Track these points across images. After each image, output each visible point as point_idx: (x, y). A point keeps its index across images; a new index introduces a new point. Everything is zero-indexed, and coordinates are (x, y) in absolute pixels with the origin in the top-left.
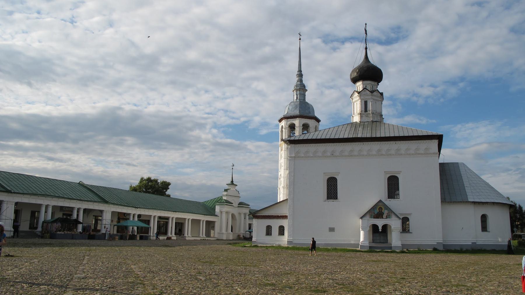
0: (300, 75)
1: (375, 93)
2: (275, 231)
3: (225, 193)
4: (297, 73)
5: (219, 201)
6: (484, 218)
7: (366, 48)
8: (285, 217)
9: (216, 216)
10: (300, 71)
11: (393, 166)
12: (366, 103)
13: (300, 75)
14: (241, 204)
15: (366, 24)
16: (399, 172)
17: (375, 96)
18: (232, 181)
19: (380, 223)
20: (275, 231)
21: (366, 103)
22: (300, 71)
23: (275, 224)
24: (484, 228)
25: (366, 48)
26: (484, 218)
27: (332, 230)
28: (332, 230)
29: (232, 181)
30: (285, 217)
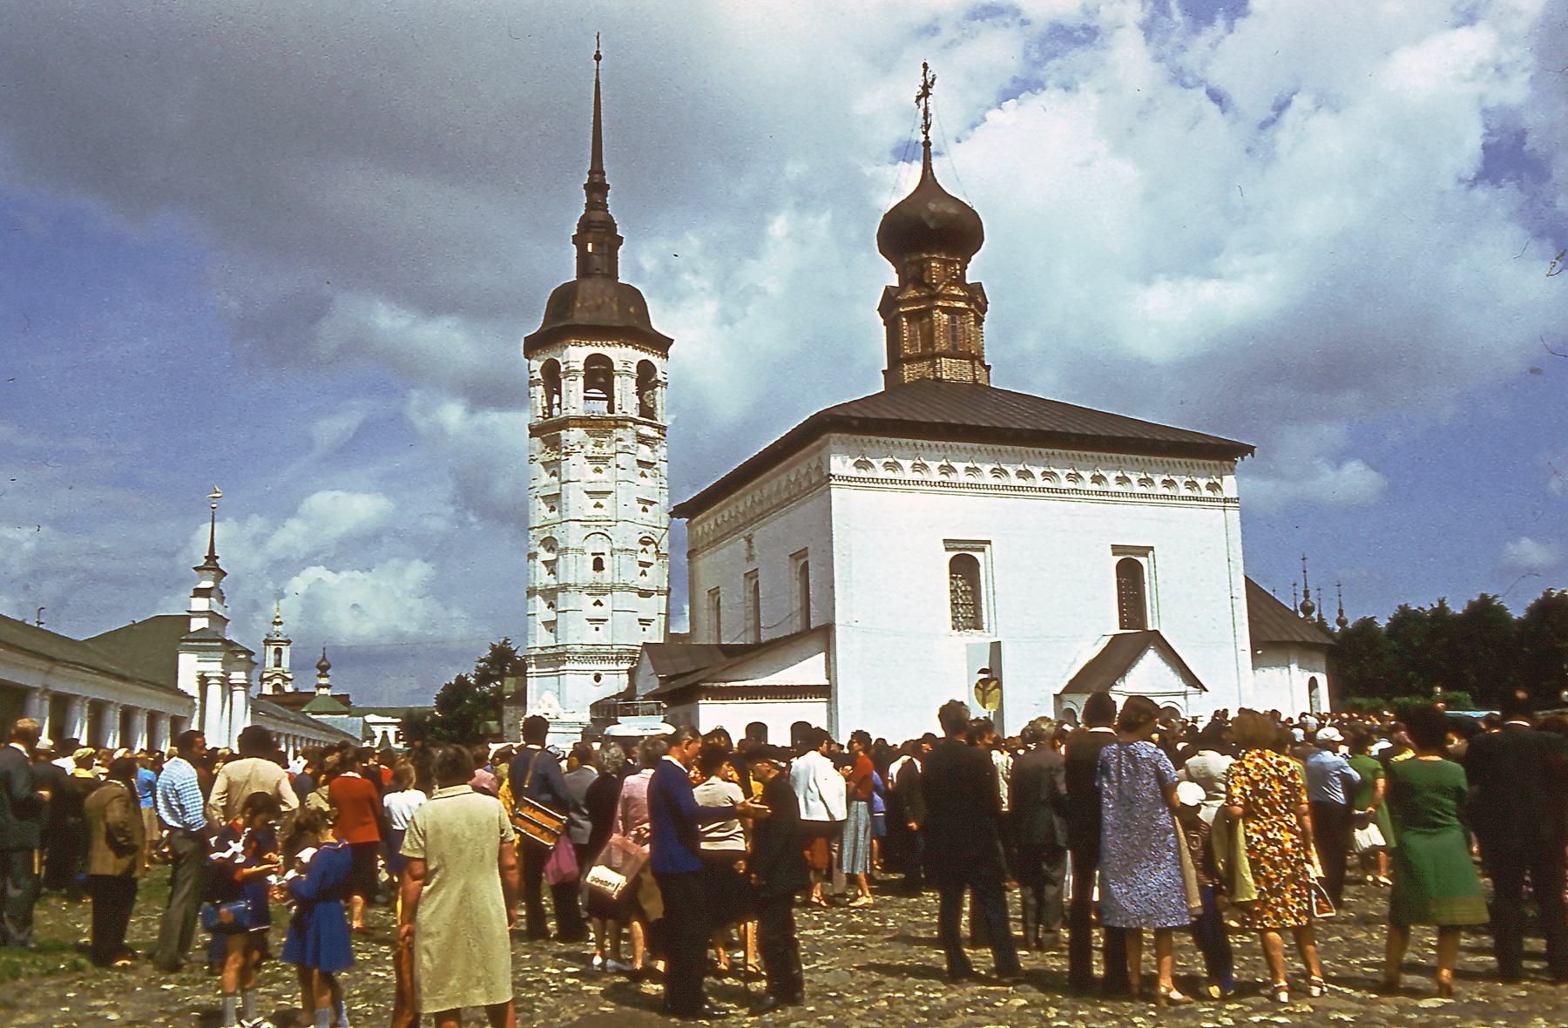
0: (597, 188)
13: (597, 188)
16: (1145, 551)
18: (212, 557)
29: (212, 557)
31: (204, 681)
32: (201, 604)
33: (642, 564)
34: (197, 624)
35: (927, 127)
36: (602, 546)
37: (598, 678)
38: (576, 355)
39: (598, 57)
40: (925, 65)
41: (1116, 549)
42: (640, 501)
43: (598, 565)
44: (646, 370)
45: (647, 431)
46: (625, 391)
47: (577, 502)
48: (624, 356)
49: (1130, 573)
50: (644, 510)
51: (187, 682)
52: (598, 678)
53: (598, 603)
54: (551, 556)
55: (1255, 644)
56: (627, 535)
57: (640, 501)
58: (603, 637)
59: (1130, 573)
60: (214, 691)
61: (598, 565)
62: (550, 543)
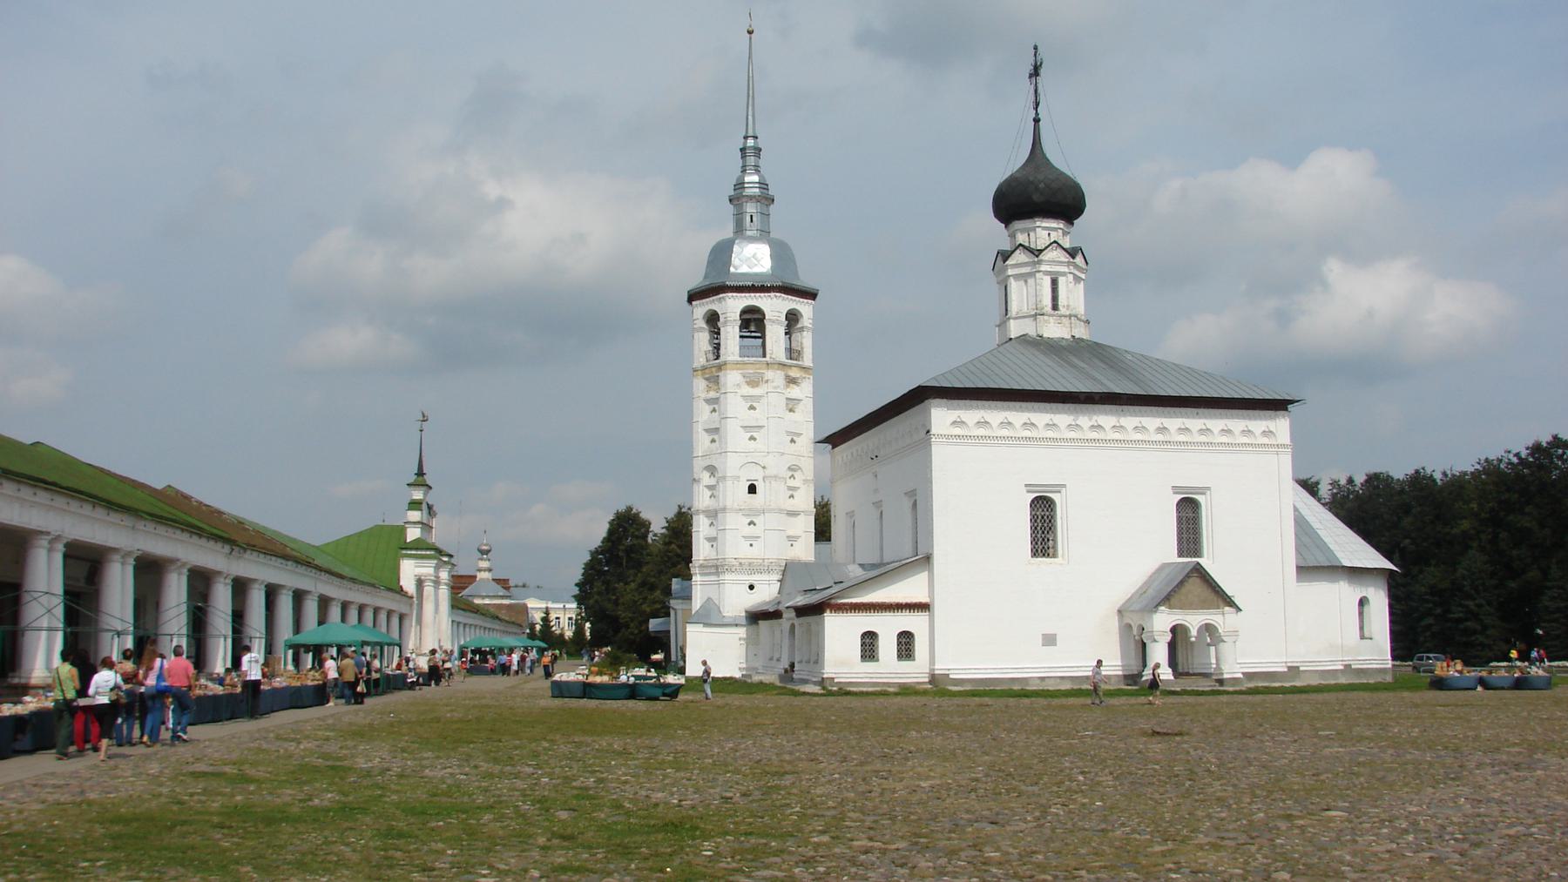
1: (1079, 260)
2: (887, 647)
6: (1363, 602)
7: (1037, 121)
11: (1190, 471)
12: (1054, 283)
15: (1036, 48)
18: (420, 473)
19: (1194, 621)
20: (887, 647)
21: (1054, 283)
23: (888, 628)
25: (1037, 121)
27: (1049, 640)
28: (1049, 640)
29: (420, 473)
31: (420, 583)
32: (415, 515)
33: (790, 488)
34: (413, 534)
35: (1037, 104)
36: (755, 475)
37: (751, 587)
38: (732, 306)
39: (750, 32)
40: (1036, 48)
41: (1176, 489)
42: (789, 433)
43: (752, 489)
44: (792, 318)
45: (794, 373)
46: (775, 333)
47: (736, 438)
49: (1189, 510)
50: (793, 441)
51: (408, 584)
52: (751, 587)
53: (751, 523)
54: (712, 481)
56: (777, 466)
57: (789, 433)
58: (756, 552)
59: (1189, 510)
60: (428, 589)
61: (752, 489)
62: (712, 470)
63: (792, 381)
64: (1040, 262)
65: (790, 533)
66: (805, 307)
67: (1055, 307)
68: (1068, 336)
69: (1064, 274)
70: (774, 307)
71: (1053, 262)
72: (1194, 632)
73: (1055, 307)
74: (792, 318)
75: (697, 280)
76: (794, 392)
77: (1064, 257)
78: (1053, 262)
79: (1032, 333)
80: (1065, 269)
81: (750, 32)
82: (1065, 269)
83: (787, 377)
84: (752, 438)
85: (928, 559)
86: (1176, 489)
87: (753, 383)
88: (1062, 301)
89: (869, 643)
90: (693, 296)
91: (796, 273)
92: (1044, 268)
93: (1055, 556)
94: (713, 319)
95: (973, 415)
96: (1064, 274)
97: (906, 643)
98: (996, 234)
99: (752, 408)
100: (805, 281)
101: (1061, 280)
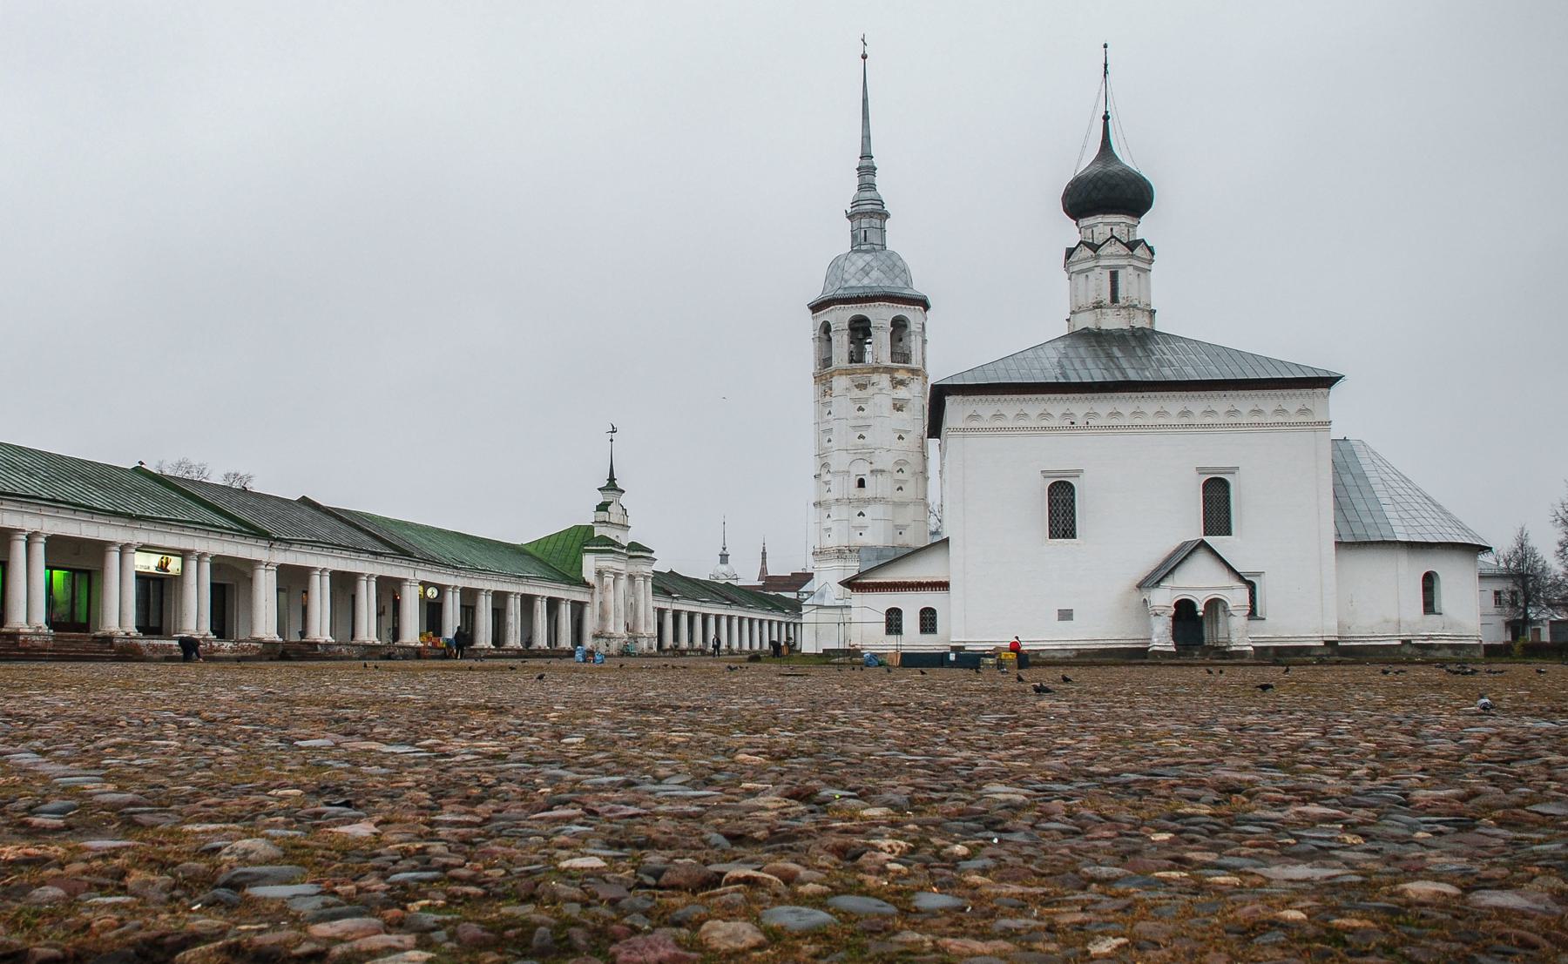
0: (867, 170)
1: (1139, 251)
2: (911, 622)
3: (602, 516)
4: (856, 162)
5: (583, 539)
6: (1429, 580)
7: (1106, 118)
8: (944, 586)
9: (585, 584)
10: (866, 155)
11: (1217, 452)
12: (1114, 276)
13: (867, 170)
14: (637, 551)
17: (1138, 258)
18: (612, 479)
20: (911, 622)
21: (1114, 276)
22: (866, 155)
23: (912, 605)
24: (1429, 606)
25: (1106, 118)
26: (1429, 580)
27: (1066, 615)
28: (1066, 615)
29: (612, 479)
30: (944, 586)
33: (897, 481)
38: (840, 317)
39: (864, 57)
42: (895, 431)
43: (861, 483)
44: (899, 325)
45: (900, 375)
48: (879, 316)
50: (900, 438)
51: (589, 574)
53: (861, 514)
55: (1340, 545)
57: (895, 431)
61: (861, 483)
63: (902, 383)
64: (1097, 257)
65: (899, 522)
66: (911, 314)
67: (1114, 299)
68: (1126, 327)
69: (1123, 267)
70: (879, 316)
71: (1111, 256)
72: (1200, 608)
73: (1114, 299)
74: (899, 325)
75: (816, 295)
76: (902, 393)
77: (1124, 251)
78: (1111, 256)
79: (1092, 326)
80: (1125, 262)
81: (864, 57)
82: (1125, 262)
83: (893, 379)
84: (861, 437)
85: (947, 540)
86: (1201, 471)
87: (862, 387)
88: (1121, 294)
89: (893, 621)
90: (816, 307)
91: (908, 284)
92: (1103, 262)
93: (1074, 537)
94: (826, 328)
95: (986, 407)
96: (1123, 267)
97: (928, 620)
98: (1070, 232)
99: (861, 409)
100: (919, 288)
101: (1121, 274)
